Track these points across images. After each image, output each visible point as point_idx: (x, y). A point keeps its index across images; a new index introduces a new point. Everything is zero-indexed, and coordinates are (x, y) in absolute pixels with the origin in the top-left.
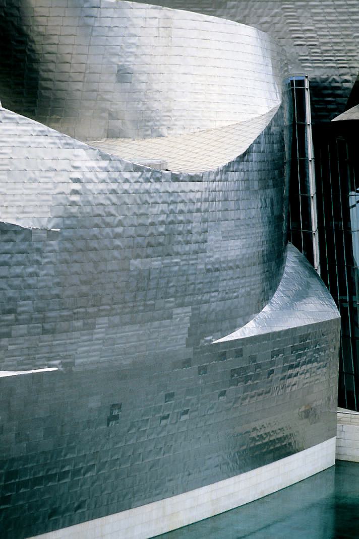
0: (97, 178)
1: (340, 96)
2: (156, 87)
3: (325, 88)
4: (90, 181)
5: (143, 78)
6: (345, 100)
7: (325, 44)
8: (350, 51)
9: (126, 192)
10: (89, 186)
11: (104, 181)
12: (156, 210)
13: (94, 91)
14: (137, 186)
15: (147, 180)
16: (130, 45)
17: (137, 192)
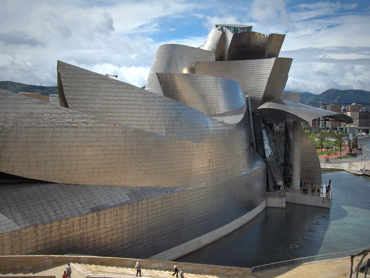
0: (212, 126)
1: (258, 102)
2: (214, 99)
3: (254, 100)
4: (210, 127)
5: (210, 97)
6: (260, 103)
7: (253, 87)
8: (260, 89)
9: (219, 130)
10: (210, 129)
11: (213, 127)
12: (226, 135)
13: (196, 101)
14: (221, 128)
15: (224, 126)
16: (206, 88)
17: (221, 130)
